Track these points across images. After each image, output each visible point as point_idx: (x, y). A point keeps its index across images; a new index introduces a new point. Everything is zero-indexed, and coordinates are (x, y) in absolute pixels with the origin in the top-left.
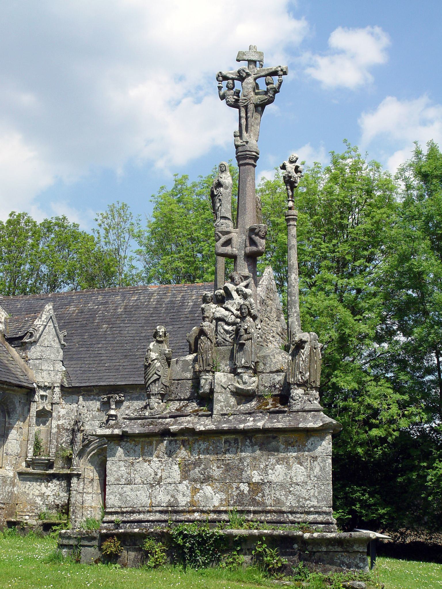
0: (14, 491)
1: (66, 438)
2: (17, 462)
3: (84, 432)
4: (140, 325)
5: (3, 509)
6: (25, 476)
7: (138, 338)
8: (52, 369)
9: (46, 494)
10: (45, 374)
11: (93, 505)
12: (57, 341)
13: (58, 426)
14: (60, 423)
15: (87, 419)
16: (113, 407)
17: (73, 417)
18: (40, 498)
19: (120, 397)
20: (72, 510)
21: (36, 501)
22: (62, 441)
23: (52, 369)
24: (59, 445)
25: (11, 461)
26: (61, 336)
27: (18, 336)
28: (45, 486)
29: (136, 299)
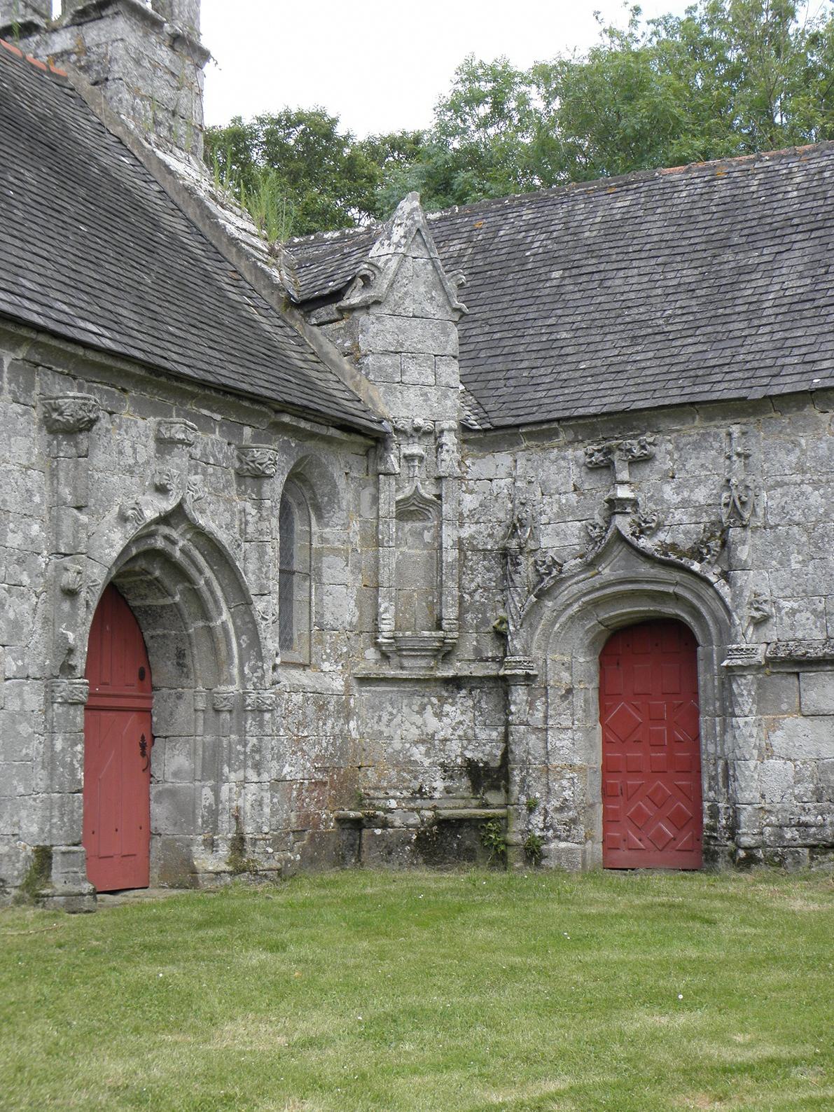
0: (349, 731)
1: (482, 574)
2: (351, 648)
3: (538, 556)
4: (660, 260)
5: (325, 784)
6: (378, 689)
7: (659, 291)
8: (431, 380)
9: (439, 736)
10: (412, 395)
11: (577, 761)
12: (440, 299)
13: (459, 543)
14: (466, 532)
15: (544, 519)
16: (624, 475)
17: (501, 515)
18: (422, 749)
19: (643, 447)
20: (517, 779)
21: (411, 756)
22: (473, 586)
23: (431, 380)
24: (467, 597)
25: (334, 649)
26: (451, 285)
27: (326, 292)
28: (436, 714)
29: (628, 203)
